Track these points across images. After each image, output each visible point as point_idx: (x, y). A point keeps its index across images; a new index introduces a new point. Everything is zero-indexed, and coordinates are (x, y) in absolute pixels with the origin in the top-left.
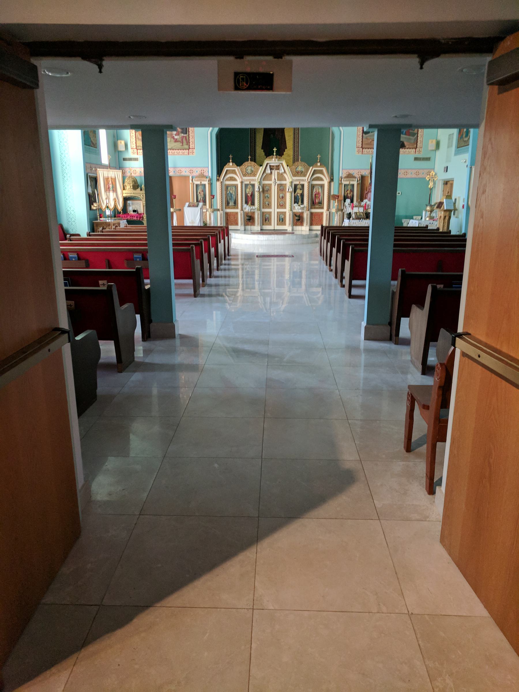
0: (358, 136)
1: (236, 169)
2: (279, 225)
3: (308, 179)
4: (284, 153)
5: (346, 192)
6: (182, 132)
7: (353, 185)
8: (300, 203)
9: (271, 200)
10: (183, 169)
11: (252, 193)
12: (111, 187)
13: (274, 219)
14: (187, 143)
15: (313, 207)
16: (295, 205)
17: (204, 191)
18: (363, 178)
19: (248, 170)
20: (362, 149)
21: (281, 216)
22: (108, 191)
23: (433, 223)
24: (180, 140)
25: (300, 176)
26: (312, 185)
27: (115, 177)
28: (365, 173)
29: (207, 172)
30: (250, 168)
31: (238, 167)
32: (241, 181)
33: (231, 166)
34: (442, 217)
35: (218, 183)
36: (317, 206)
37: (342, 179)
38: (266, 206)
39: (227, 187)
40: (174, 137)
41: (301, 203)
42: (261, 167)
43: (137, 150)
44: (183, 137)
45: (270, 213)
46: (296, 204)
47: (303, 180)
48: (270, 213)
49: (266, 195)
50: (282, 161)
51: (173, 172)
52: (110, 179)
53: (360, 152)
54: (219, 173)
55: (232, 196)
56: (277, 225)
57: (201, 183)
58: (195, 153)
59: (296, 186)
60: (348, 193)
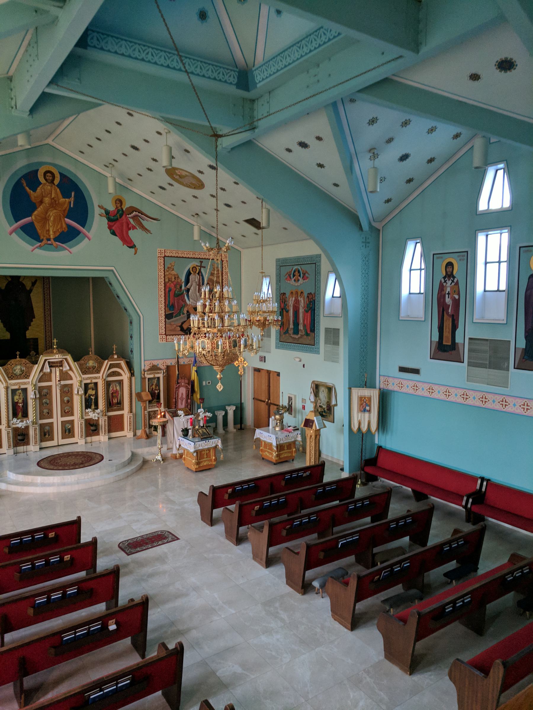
0: (160, 321)
4: (32, 323)
7: (159, 378)
8: (93, 407)
9: (52, 407)
11: (23, 401)
13: (57, 430)
15: (110, 409)
16: (87, 411)
18: (168, 367)
19: (17, 371)
20: (165, 336)
21: (67, 425)
25: (92, 373)
26: (107, 382)
28: (171, 363)
30: (19, 367)
32: (5, 386)
34: (313, 437)
36: (115, 408)
37: (146, 373)
38: (44, 415)
42: (37, 366)
45: (51, 425)
46: (89, 410)
47: (96, 378)
49: (44, 401)
53: (163, 340)
56: (62, 438)
59: (86, 385)
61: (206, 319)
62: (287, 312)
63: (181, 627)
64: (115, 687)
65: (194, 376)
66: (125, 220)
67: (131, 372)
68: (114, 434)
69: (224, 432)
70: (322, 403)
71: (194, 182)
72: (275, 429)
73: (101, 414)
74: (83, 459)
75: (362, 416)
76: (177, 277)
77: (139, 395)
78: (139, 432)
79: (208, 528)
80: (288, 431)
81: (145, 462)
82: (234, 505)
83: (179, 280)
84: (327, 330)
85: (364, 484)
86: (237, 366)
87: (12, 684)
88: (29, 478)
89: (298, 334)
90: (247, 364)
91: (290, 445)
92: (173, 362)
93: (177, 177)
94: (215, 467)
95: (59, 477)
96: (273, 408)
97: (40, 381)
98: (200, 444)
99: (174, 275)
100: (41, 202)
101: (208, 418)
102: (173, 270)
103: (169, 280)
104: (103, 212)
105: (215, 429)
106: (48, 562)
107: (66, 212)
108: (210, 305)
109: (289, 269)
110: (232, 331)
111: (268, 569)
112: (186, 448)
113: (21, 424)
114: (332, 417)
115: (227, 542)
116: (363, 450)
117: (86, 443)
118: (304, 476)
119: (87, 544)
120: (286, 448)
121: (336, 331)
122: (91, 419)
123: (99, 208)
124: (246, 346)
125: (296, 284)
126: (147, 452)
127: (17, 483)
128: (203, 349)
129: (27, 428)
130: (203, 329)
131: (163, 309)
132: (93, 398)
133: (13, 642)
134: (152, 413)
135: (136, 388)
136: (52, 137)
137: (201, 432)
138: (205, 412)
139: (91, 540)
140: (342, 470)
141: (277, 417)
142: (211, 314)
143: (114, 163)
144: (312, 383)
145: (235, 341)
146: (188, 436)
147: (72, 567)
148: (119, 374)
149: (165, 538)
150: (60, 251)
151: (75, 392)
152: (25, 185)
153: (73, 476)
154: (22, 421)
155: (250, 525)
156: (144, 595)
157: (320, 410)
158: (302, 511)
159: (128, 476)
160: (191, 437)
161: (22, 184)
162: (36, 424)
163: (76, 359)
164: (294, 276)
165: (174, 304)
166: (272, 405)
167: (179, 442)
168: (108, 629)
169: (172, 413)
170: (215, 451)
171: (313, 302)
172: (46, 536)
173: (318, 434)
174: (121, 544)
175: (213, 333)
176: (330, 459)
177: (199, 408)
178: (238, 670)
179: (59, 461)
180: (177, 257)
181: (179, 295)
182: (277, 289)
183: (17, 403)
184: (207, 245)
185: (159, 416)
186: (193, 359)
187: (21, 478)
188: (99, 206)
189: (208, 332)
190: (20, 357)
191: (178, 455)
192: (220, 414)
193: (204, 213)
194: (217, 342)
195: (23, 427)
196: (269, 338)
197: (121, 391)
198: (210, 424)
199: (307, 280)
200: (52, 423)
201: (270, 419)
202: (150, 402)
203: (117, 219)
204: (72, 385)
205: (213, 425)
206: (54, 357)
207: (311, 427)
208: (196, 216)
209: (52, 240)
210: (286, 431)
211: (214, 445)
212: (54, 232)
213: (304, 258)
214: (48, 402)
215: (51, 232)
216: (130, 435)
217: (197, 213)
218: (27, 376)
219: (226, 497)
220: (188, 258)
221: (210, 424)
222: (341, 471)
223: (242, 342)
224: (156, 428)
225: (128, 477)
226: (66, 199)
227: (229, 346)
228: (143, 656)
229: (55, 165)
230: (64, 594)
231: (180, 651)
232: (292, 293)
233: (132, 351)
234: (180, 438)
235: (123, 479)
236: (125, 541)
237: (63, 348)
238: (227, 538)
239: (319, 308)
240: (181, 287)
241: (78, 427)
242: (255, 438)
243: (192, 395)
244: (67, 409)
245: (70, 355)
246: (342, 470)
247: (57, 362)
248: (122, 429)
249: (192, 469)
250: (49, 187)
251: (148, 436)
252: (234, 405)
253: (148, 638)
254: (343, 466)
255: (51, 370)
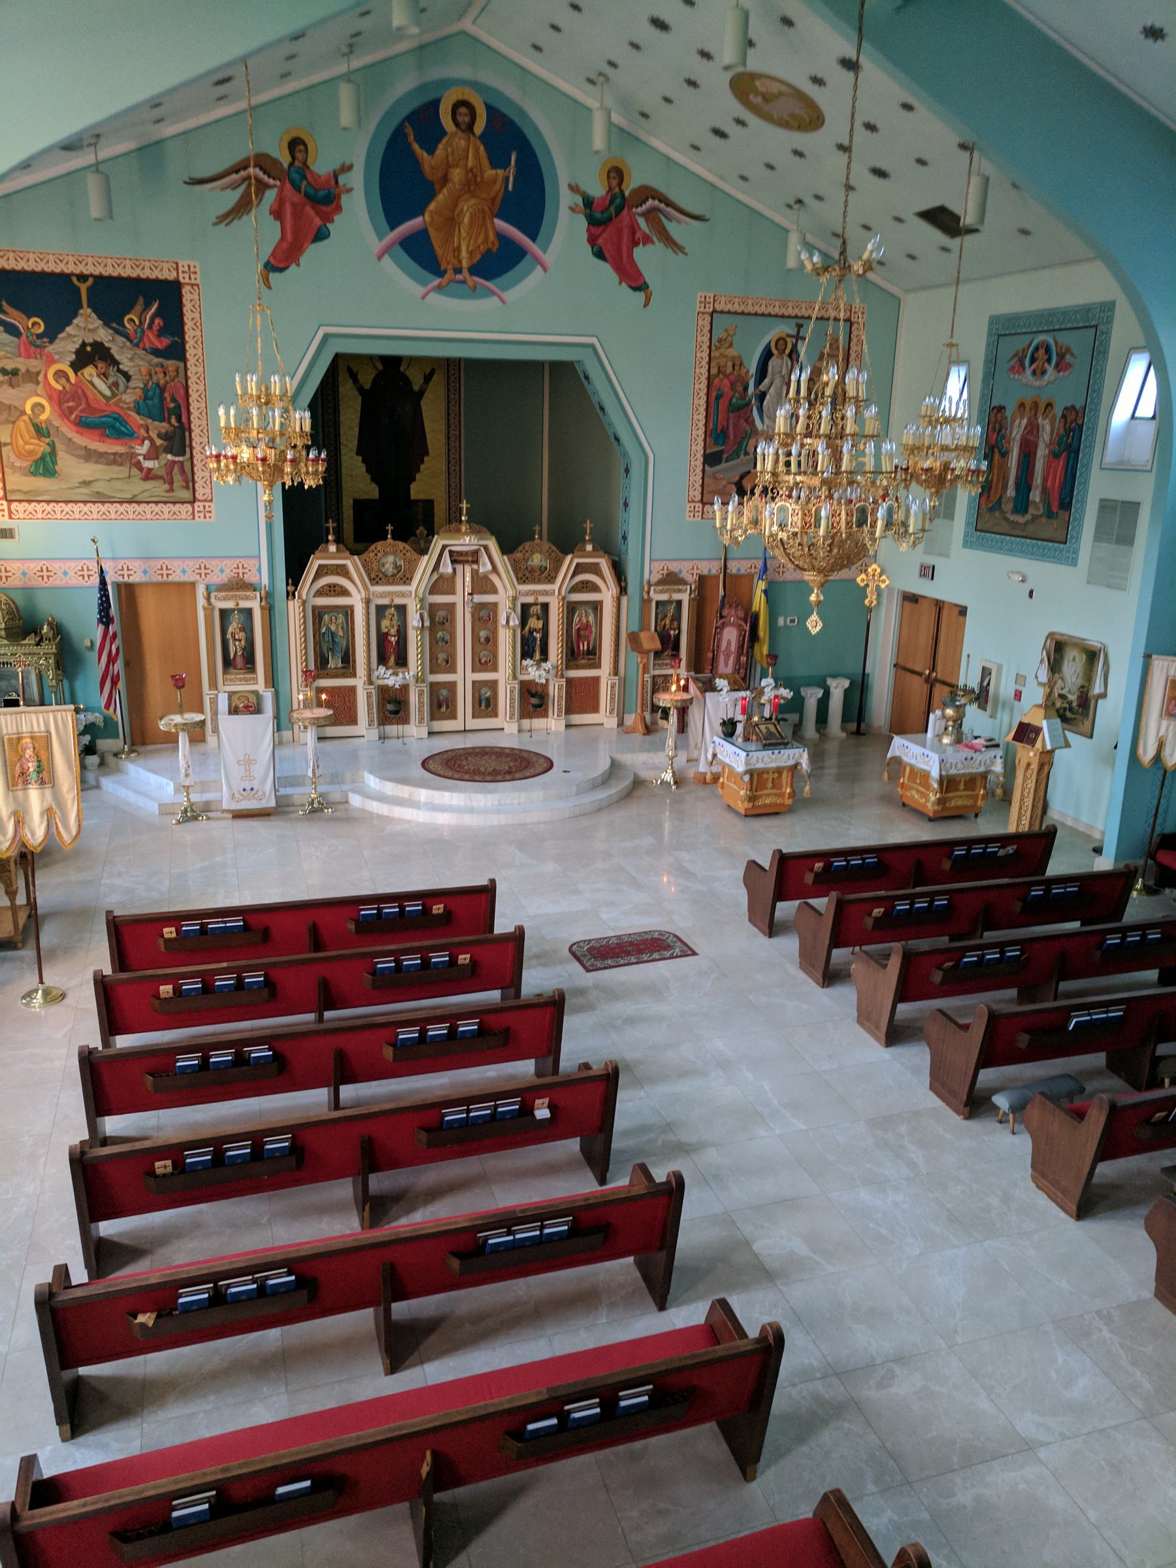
0: (692, 470)
1: (348, 562)
2: (479, 717)
3: (560, 589)
5: (662, 620)
6: (169, 450)
8: (537, 656)
9: (455, 650)
10: (175, 565)
11: (398, 631)
12: (31, 770)
13: (464, 701)
14: (187, 483)
15: (572, 663)
16: (525, 663)
17: (248, 628)
18: (702, 580)
19: (387, 566)
20: (701, 506)
21: (484, 690)
22: (20, 787)
23: (972, 758)
24: (162, 472)
25: (539, 582)
26: (569, 603)
27: (48, 732)
28: (710, 570)
29: (254, 571)
30: (391, 559)
31: (356, 557)
33: (333, 553)
34: (1035, 767)
35: (291, 603)
36: (583, 661)
37: (652, 588)
38: (439, 666)
39: (319, 614)
40: (139, 462)
41: (541, 654)
42: (426, 557)
43: (10, 502)
44: (174, 462)
45: (452, 686)
48: (452, 686)
49: (440, 634)
50: (487, 539)
51: (139, 572)
52: (28, 740)
53: (696, 515)
54: (294, 572)
55: (337, 640)
56: (474, 717)
57: (238, 604)
58: (212, 515)
59: (525, 608)
60: (665, 625)
61: (794, 451)
62: (1005, 455)
63: (684, 1137)
64: (538, 1233)
65: (759, 602)
66: (626, 221)
67: (620, 586)
68: (577, 719)
69: (817, 736)
70: (1067, 689)
71: (798, 109)
72: (940, 741)
73: (553, 672)
74: (512, 764)
75: (1171, 728)
76: (738, 363)
77: (634, 639)
78: (630, 719)
79: (762, 940)
80: (971, 747)
81: (638, 783)
82: (825, 900)
83: (743, 371)
84: (1106, 506)
85: (1148, 891)
86: (862, 585)
87: (350, 1179)
88: (404, 791)
89: (1027, 512)
90: (887, 582)
91: (973, 781)
92: (712, 568)
93: (758, 100)
94: (790, 810)
95: (462, 796)
96: (940, 692)
97: (431, 593)
98: (760, 757)
99: (733, 358)
100: (445, 179)
101: (782, 701)
102: (731, 345)
103: (719, 371)
104: (579, 201)
105: (798, 728)
106: (426, 963)
107: (498, 202)
108: (809, 417)
109: (1020, 343)
110: (858, 484)
111: (892, 1049)
112: (727, 761)
113: (392, 678)
114: (1088, 723)
115: (802, 976)
116: (1161, 810)
117: (519, 731)
118: (999, 854)
119: (505, 938)
120: (962, 787)
121: (1131, 508)
122: (532, 682)
123: (569, 191)
124: (889, 525)
125: (1037, 384)
126: (644, 763)
127: (382, 798)
128: (782, 526)
129: (405, 688)
130: (786, 478)
131: (700, 440)
132: (538, 636)
133: (358, 1103)
134: (660, 681)
135: (629, 623)
136: (474, 11)
137: (764, 730)
138: (776, 687)
139: (512, 930)
140: (1098, 851)
141: (949, 712)
142: (809, 441)
143: (609, 71)
144: (1047, 638)
145: (862, 511)
146: (734, 737)
147: (473, 979)
148: (595, 588)
149: (668, 947)
150: (482, 297)
151: (502, 620)
152: (412, 137)
153: (489, 796)
154: (396, 674)
155: (857, 948)
156: (610, 1062)
157: (1058, 704)
158: (986, 934)
159: (599, 809)
160: (740, 740)
161: (406, 136)
162: (423, 681)
163: (506, 549)
164: (1033, 360)
165: (728, 428)
166: (938, 685)
167: (714, 748)
168: (533, 1114)
169: (704, 683)
170: (793, 777)
171: (1077, 429)
172: (426, 911)
173: (1046, 760)
174: (574, 947)
175: (809, 488)
176: (1070, 823)
177: (764, 675)
178: (803, 1250)
179: (464, 763)
180: (743, 313)
181: (739, 409)
182: (983, 395)
183: (387, 634)
184: (815, 259)
185: (674, 688)
186: (760, 564)
187: (390, 788)
188: (571, 187)
189: (796, 484)
190: (394, 538)
191: (708, 777)
192: (812, 696)
193: (818, 198)
194: (818, 512)
195: (397, 686)
196: (947, 521)
197: (596, 628)
198: (786, 716)
199: (1067, 373)
200: (454, 684)
201: (932, 716)
202: (658, 654)
203: (610, 219)
204: (495, 605)
205: (793, 718)
206: (461, 542)
207: (1032, 742)
208: (796, 207)
209: (466, 273)
210: (967, 746)
211: (791, 762)
212: (471, 253)
213: (1065, 313)
214: (447, 637)
215: (464, 254)
216: (611, 722)
217: (801, 197)
218: (407, 580)
219: (809, 878)
220: (770, 315)
221: (786, 716)
222: (1093, 854)
223: (881, 513)
224: (665, 713)
225: (600, 810)
226: (499, 171)
227: (848, 523)
228: (602, 1181)
229: (476, 85)
230: (453, 1030)
231: (675, 1190)
232: (1022, 405)
233: (625, 538)
234: (716, 739)
235: (591, 813)
236: (585, 941)
237: (482, 521)
238: (803, 967)
239: (1091, 447)
240: (746, 389)
241: (506, 697)
242: (889, 755)
243: (751, 647)
244: (484, 655)
245: (493, 539)
246: (1098, 851)
247: (467, 553)
248: (595, 709)
249: (737, 809)
250: (463, 143)
251: (649, 730)
252: (846, 676)
253: (615, 1145)
254: (1102, 841)
255: (454, 570)
